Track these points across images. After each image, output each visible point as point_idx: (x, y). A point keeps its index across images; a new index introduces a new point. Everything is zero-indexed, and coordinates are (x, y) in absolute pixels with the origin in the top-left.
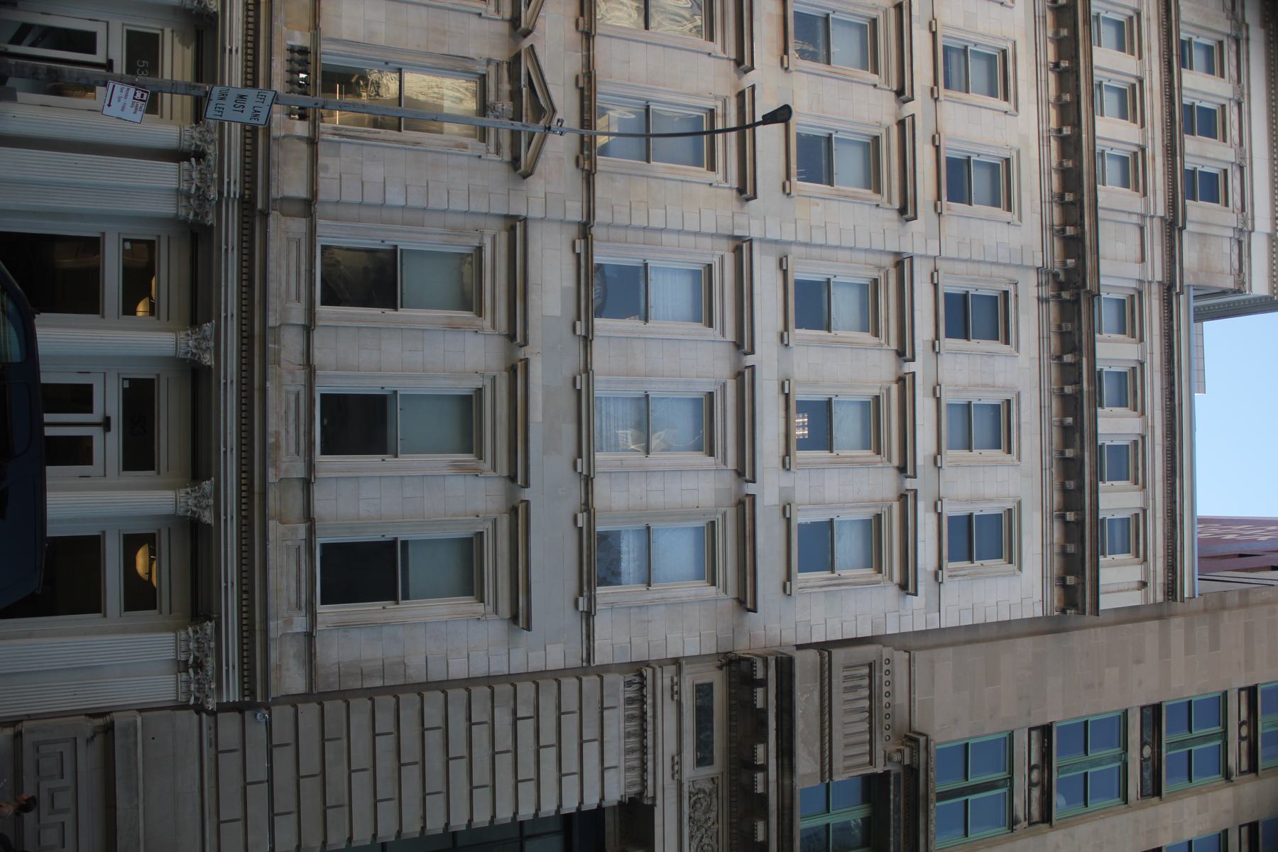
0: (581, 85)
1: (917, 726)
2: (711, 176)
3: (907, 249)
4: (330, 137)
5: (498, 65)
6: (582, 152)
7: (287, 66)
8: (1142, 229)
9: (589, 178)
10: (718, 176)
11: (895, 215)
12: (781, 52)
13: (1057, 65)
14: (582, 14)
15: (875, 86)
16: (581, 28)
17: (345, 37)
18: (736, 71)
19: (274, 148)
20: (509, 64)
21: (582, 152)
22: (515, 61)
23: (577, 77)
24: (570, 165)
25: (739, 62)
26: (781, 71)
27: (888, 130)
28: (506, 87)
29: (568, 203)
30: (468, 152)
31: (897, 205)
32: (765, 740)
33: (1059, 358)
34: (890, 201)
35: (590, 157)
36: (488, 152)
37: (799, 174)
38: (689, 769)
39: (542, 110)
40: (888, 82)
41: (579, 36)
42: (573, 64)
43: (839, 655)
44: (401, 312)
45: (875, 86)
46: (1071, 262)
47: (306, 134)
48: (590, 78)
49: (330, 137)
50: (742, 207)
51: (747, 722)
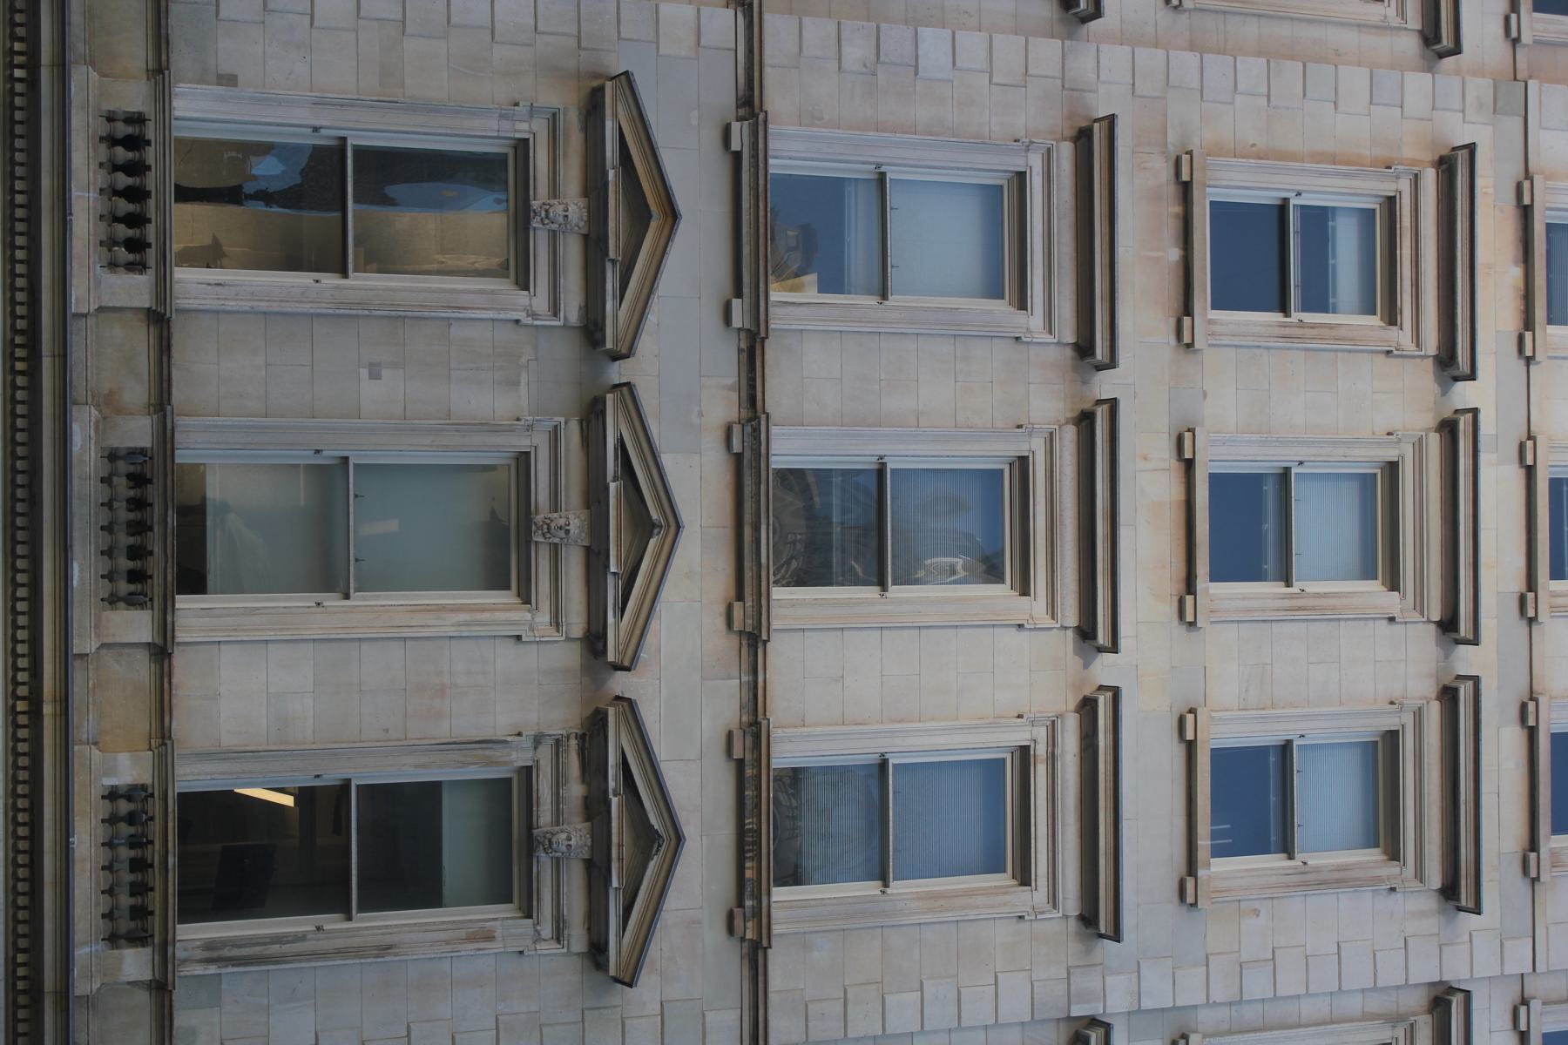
0: (737, 754)
2: (1023, 899)
3: (1456, 972)
4: (199, 970)
5: (558, 742)
6: (741, 904)
7: (101, 833)
9: (756, 956)
10: (1040, 895)
11: (1430, 902)
12: (1182, 587)
14: (740, 596)
15: (1392, 619)
16: (737, 626)
17: (228, 741)
18: (1079, 652)
19: (78, 1017)
20: (581, 738)
21: (741, 904)
22: (593, 730)
23: (730, 735)
24: (714, 933)
25: (1086, 632)
26: (1179, 630)
27: (1418, 715)
28: (575, 790)
29: (710, 1016)
30: (496, 946)
31: (1435, 879)
34: (1420, 875)
35: (757, 913)
36: (538, 938)
37: (1214, 835)
40: (1420, 605)
41: (734, 641)
42: (721, 708)
45: (1392, 619)
47: (147, 975)
48: (757, 737)
49: (199, 970)
50: (1089, 951)
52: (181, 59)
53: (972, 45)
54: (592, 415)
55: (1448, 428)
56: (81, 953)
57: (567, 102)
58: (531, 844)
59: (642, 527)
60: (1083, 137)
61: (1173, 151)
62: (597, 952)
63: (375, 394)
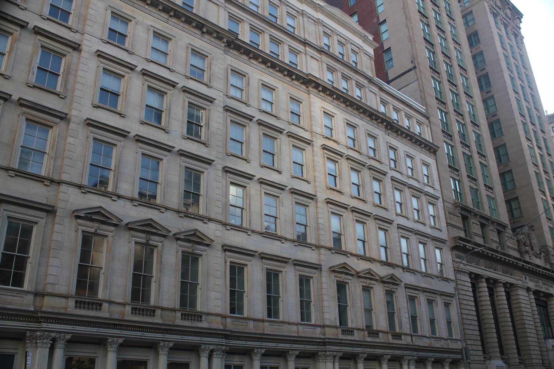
1: (452, 202)
8: (370, 91)
13: (347, 106)
22: (384, 282)
28: (387, 285)
32: (466, 245)
33: (398, 134)
38: (464, 262)
39: (392, 277)
43: (449, 221)
44: (418, 315)
46: (385, 124)
51: (464, 249)
52: (334, 324)
53: (320, 215)
54: (359, 277)
55: (348, 159)
56: (403, 343)
57: (333, 275)
58: (391, 291)
59: (369, 273)
60: (328, 203)
61: (325, 188)
62: (398, 285)
63: (359, 304)
